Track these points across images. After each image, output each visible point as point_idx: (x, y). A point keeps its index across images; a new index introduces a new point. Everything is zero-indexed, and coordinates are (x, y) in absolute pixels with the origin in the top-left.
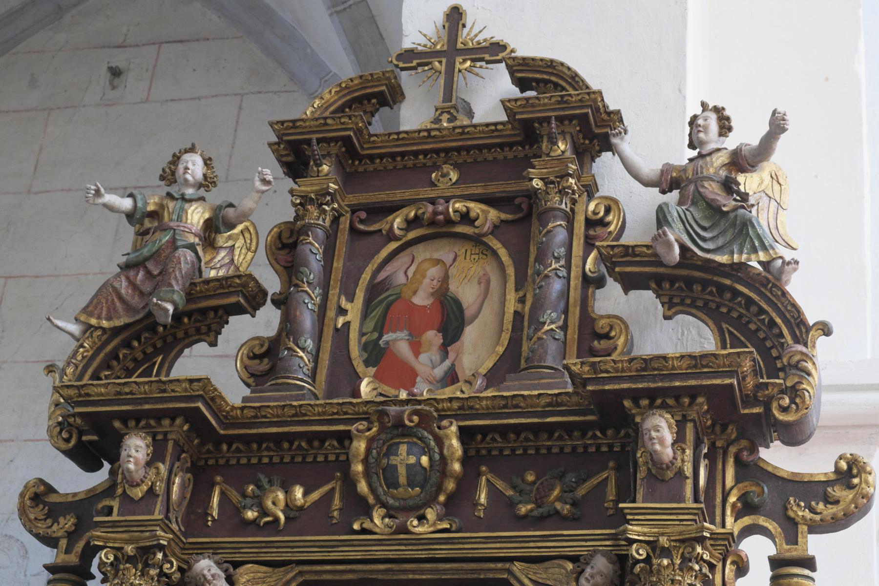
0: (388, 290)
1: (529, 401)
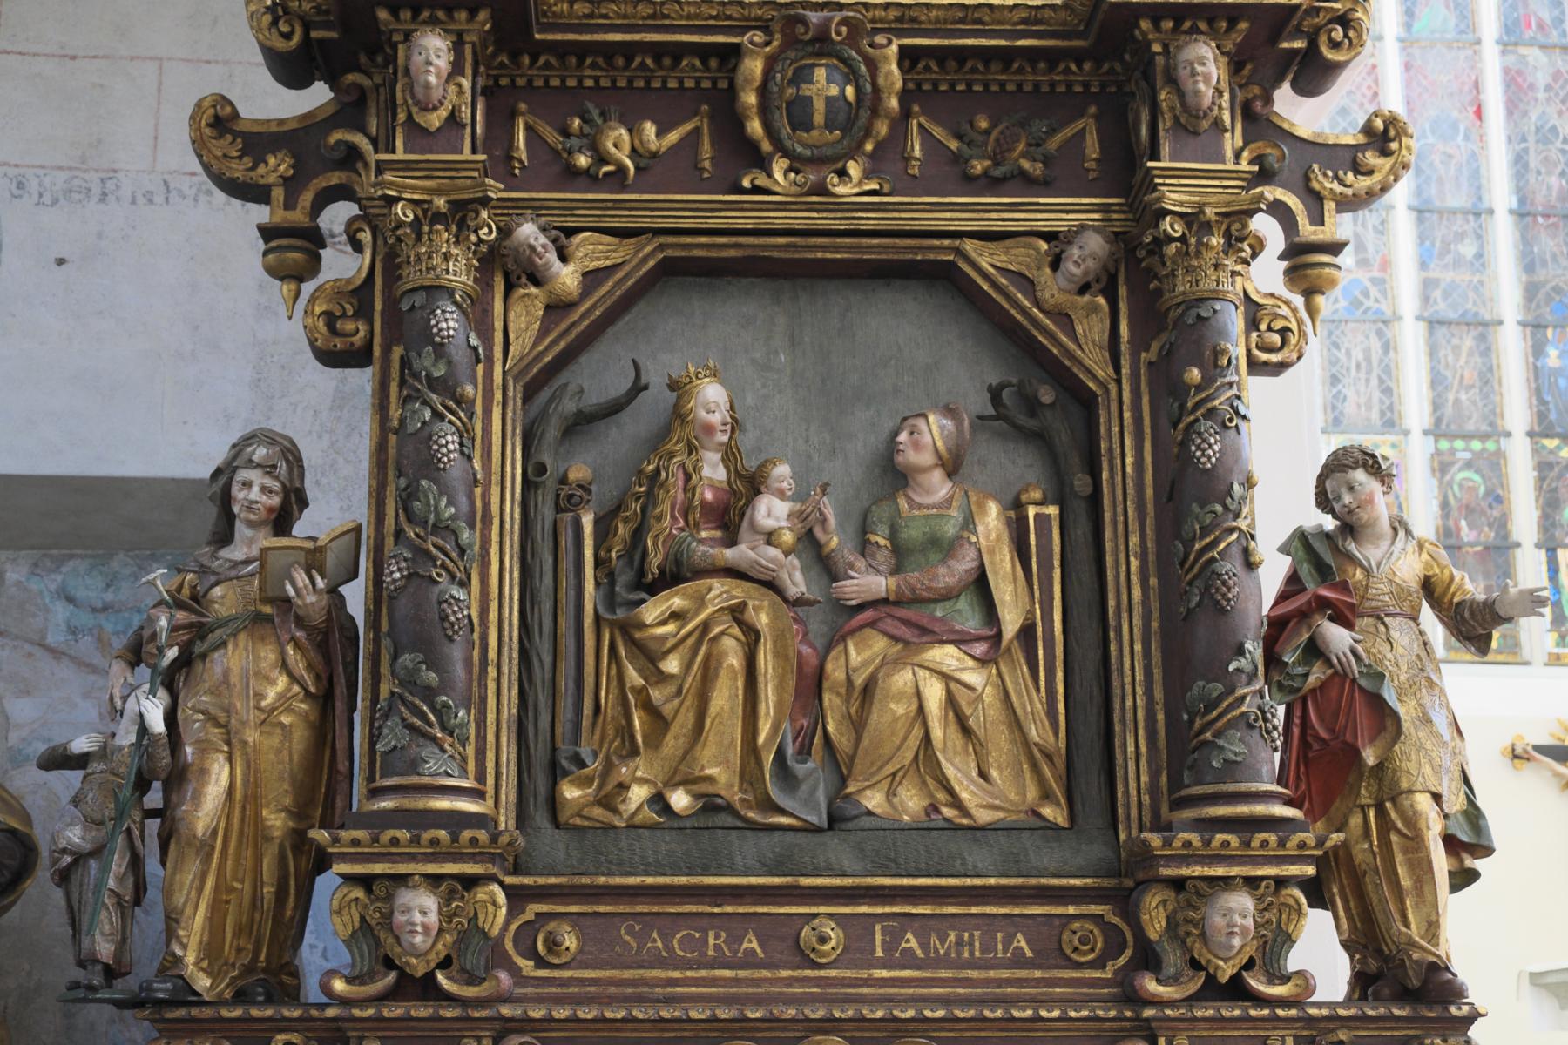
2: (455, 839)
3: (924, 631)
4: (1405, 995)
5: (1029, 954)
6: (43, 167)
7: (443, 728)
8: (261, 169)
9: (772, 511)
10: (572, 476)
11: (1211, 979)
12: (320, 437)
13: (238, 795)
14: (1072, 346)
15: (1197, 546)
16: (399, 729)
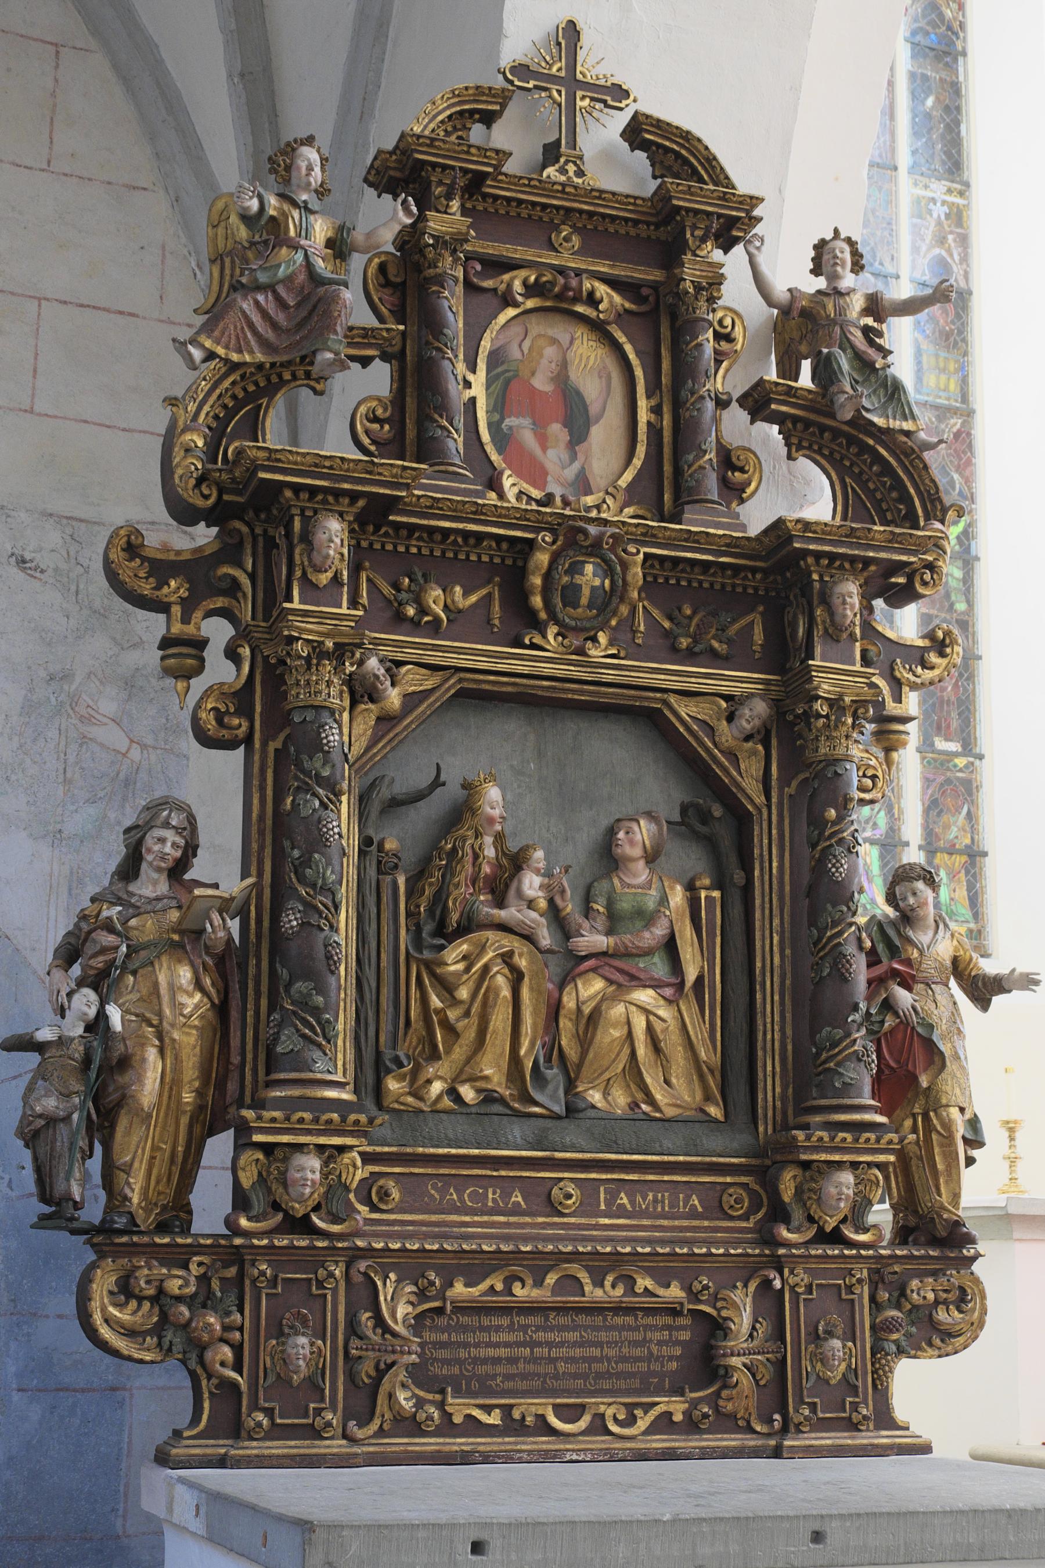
0: (503, 363)
1: (710, 539)
2: (344, 1119)
3: (633, 977)
4: (935, 1241)
5: (700, 1209)
7: (325, 1037)
8: (165, 590)
9: (531, 884)
10: (388, 846)
11: (821, 1230)
12: (11, 739)
13: (167, 1079)
14: (739, 778)
15: (829, 934)
16: (296, 1037)
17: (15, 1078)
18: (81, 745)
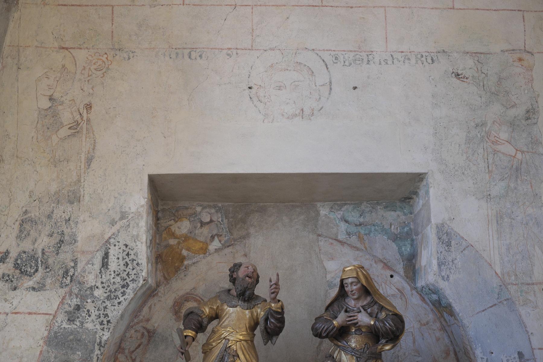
6: (344, 51)
17: (483, 311)
18: (494, 155)
